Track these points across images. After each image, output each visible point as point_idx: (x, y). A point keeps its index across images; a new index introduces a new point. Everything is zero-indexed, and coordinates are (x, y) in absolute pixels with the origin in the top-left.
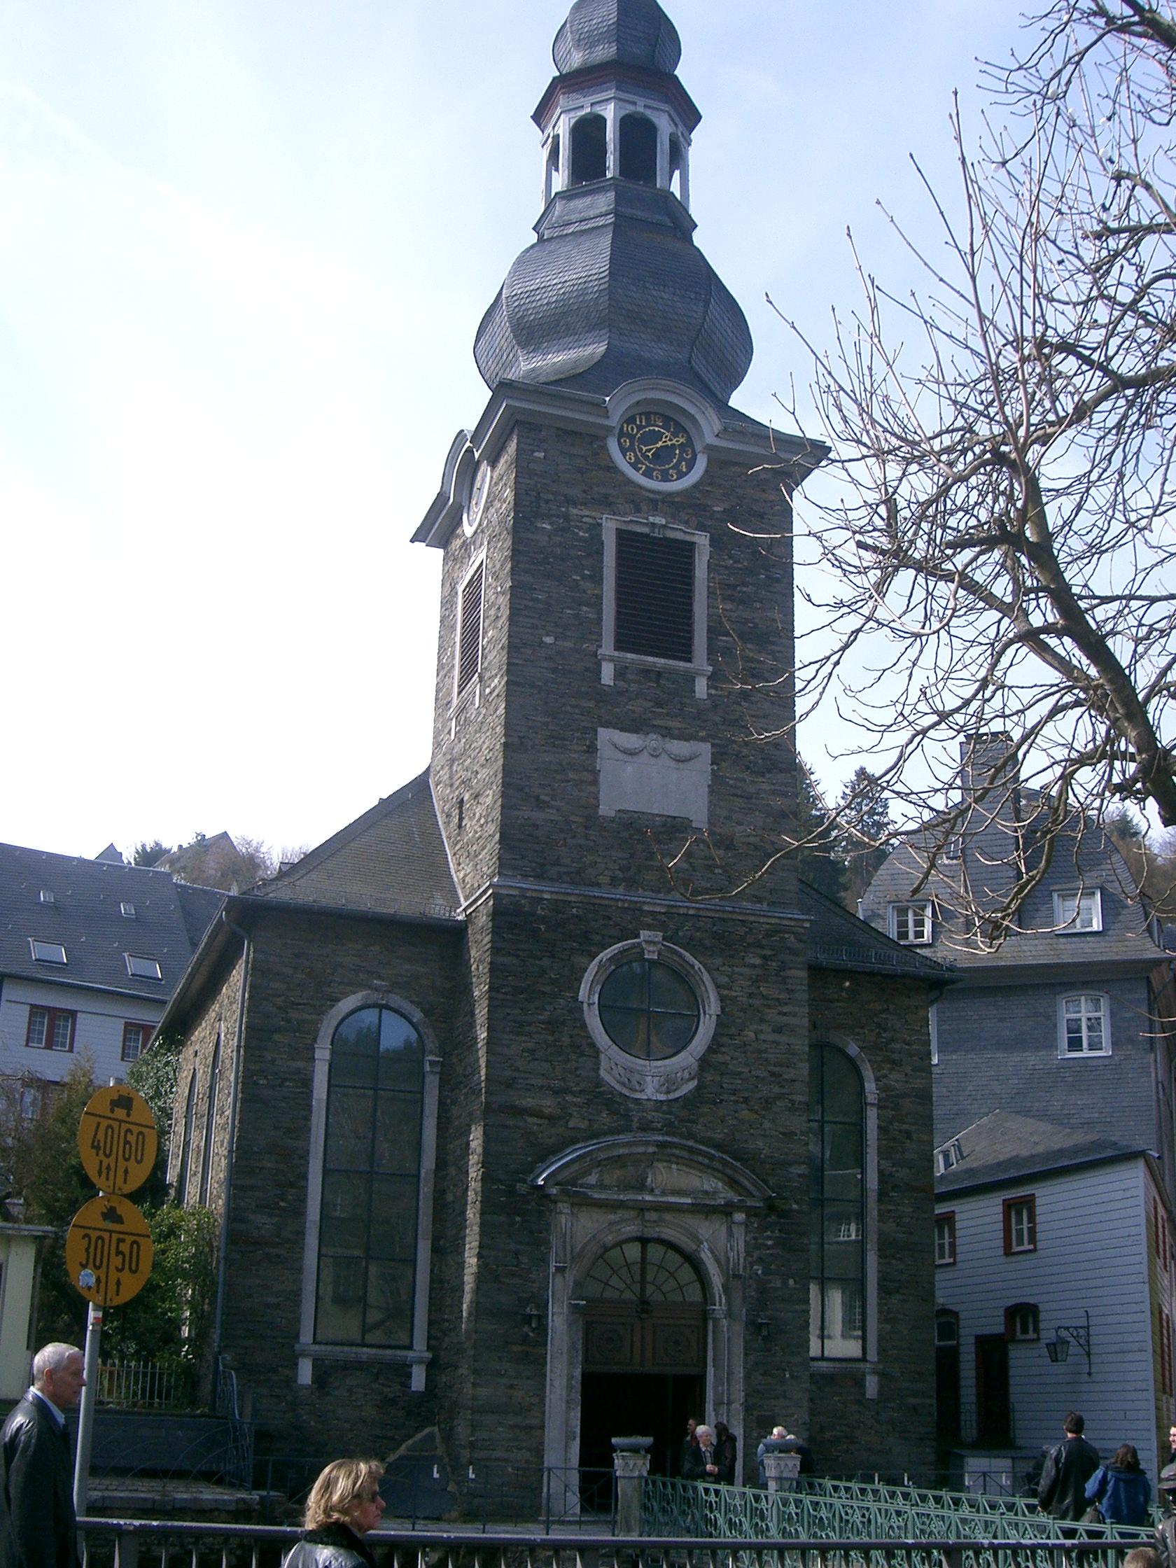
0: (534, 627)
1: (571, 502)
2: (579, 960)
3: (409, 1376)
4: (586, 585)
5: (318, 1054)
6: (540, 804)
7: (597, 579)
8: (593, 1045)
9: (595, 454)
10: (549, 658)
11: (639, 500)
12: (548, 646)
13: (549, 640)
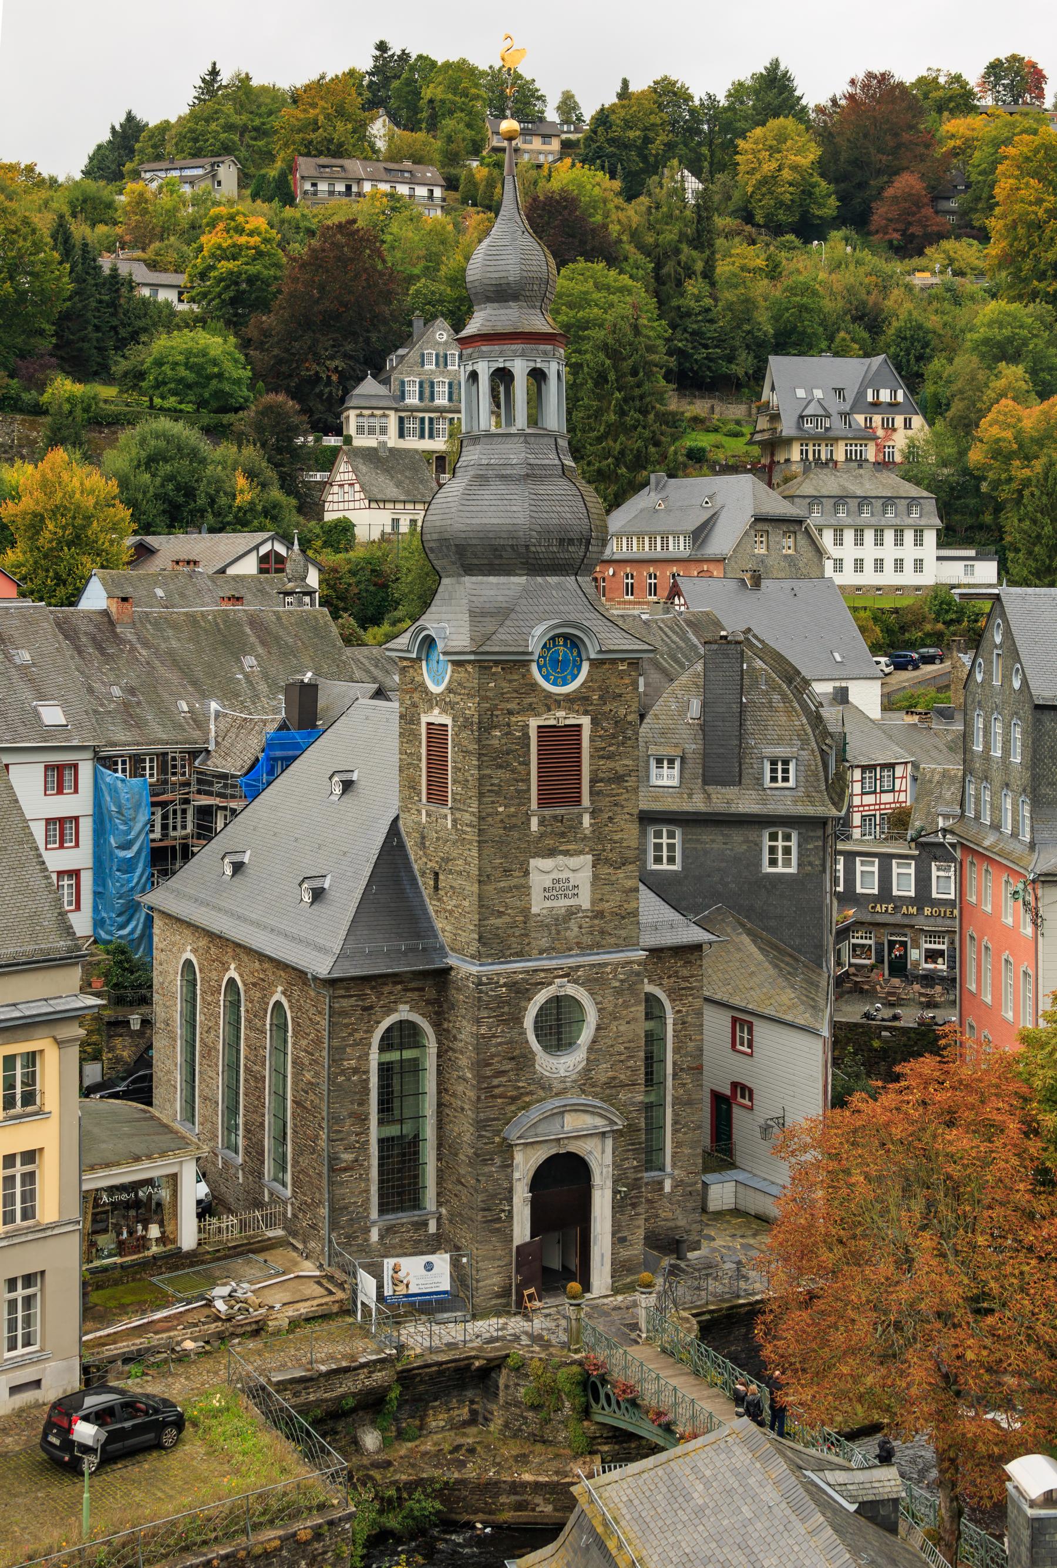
0: (493, 802)
1: (510, 713)
2: (523, 1004)
3: (426, 1225)
4: (521, 768)
5: (371, 1057)
6: (501, 914)
7: (527, 764)
8: (532, 1052)
9: (524, 676)
10: (502, 821)
11: (551, 702)
12: (501, 813)
13: (501, 809)
